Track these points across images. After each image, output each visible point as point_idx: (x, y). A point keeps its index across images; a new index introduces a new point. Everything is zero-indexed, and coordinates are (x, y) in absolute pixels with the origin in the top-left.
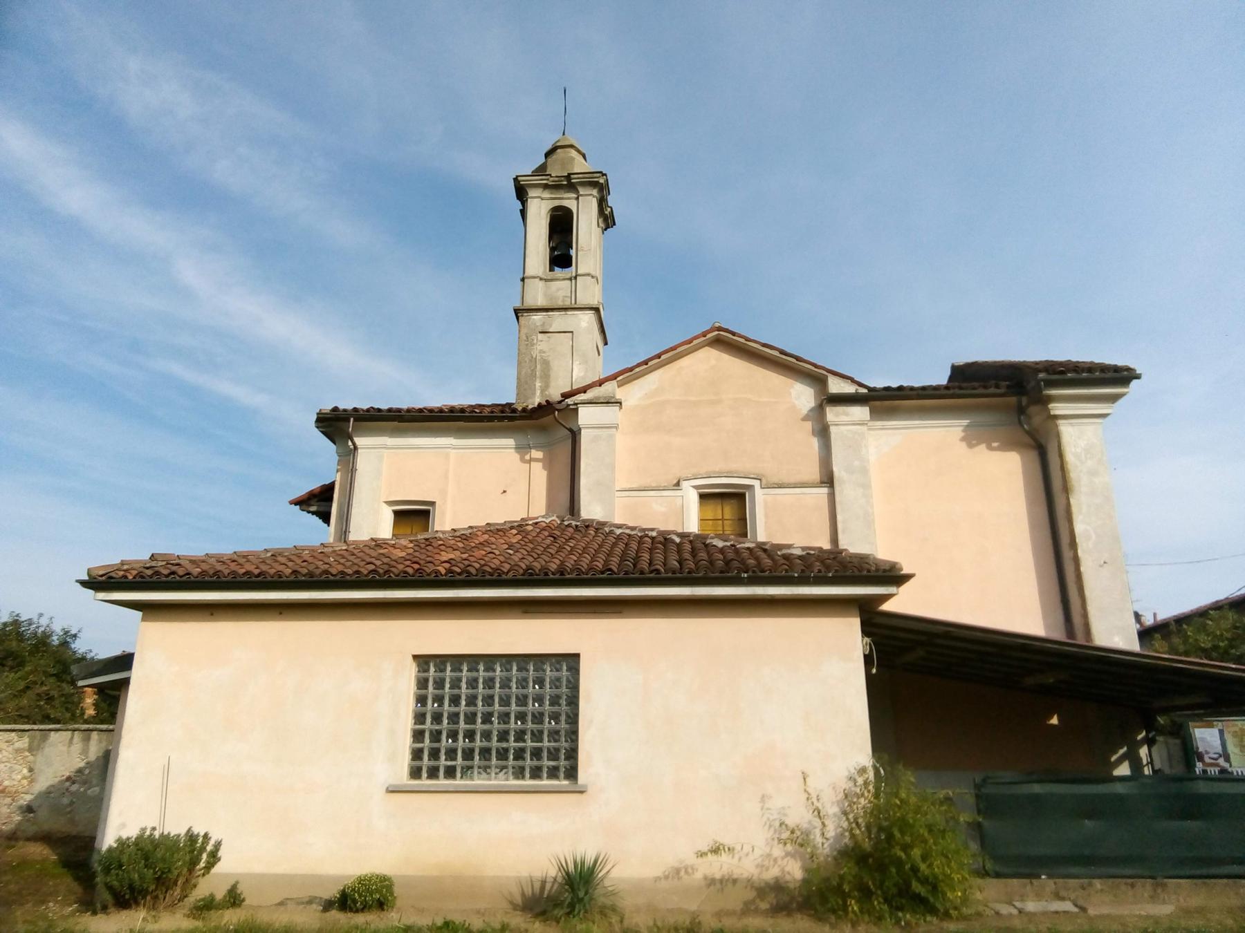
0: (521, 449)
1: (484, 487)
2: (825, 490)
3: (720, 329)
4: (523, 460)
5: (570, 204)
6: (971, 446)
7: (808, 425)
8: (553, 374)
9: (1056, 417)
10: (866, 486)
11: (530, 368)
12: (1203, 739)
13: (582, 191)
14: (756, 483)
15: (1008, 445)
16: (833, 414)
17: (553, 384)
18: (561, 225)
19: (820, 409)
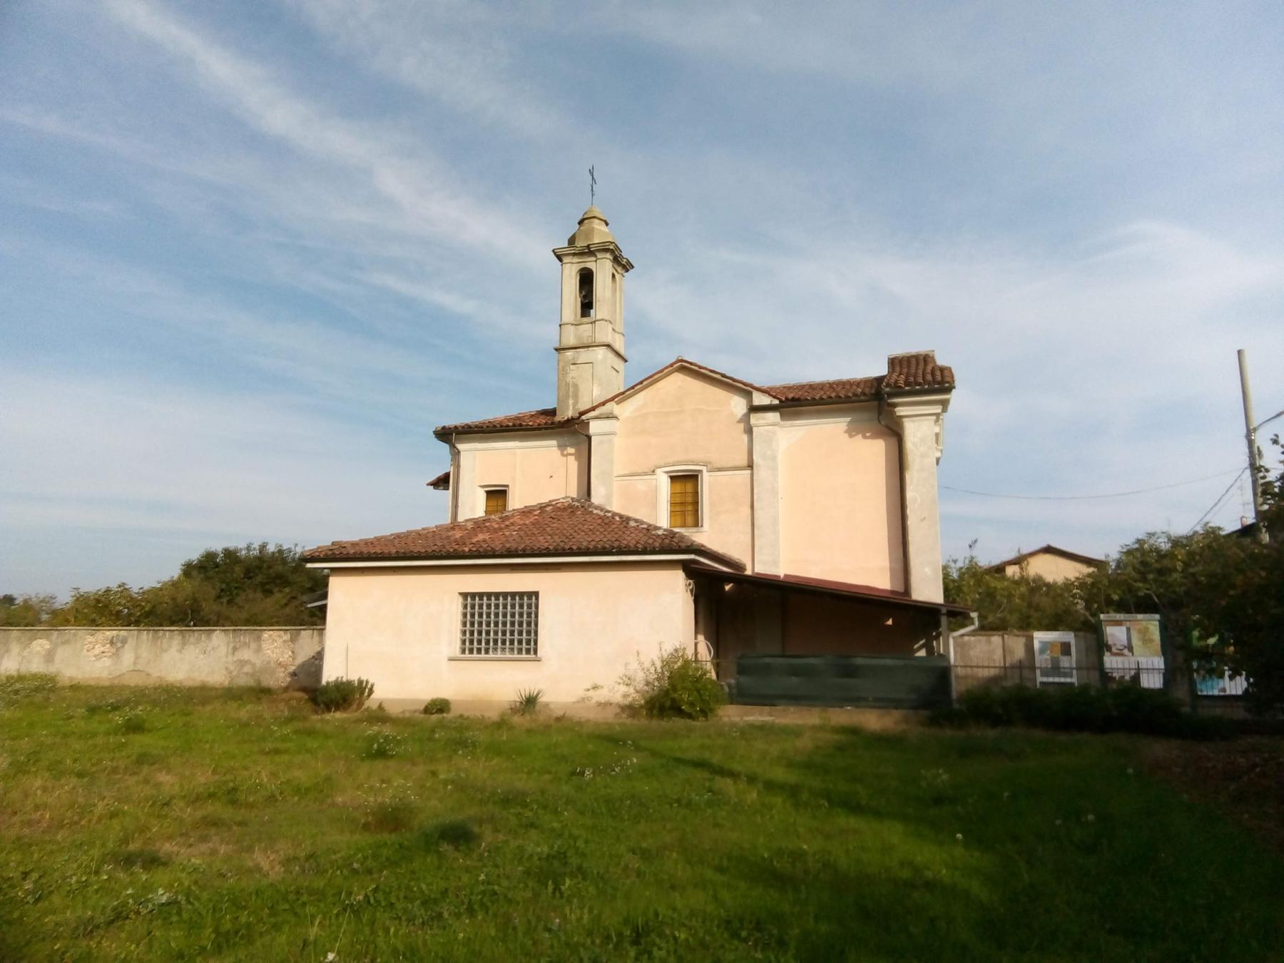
0: (562, 447)
1: (535, 475)
2: (749, 472)
3: (682, 361)
4: (563, 455)
5: (591, 265)
6: (851, 436)
7: (742, 426)
8: (580, 394)
9: (901, 417)
10: (775, 469)
11: (567, 390)
12: (1112, 635)
13: (599, 255)
14: (704, 469)
15: (876, 435)
16: (755, 419)
17: (580, 401)
18: (586, 279)
19: (746, 419)
